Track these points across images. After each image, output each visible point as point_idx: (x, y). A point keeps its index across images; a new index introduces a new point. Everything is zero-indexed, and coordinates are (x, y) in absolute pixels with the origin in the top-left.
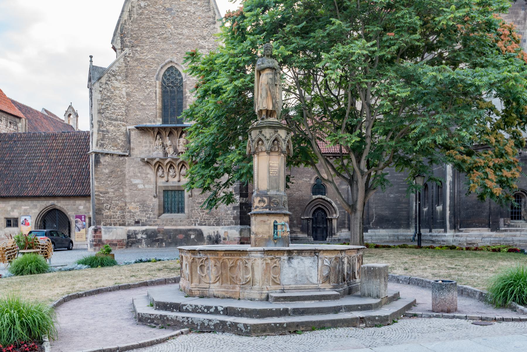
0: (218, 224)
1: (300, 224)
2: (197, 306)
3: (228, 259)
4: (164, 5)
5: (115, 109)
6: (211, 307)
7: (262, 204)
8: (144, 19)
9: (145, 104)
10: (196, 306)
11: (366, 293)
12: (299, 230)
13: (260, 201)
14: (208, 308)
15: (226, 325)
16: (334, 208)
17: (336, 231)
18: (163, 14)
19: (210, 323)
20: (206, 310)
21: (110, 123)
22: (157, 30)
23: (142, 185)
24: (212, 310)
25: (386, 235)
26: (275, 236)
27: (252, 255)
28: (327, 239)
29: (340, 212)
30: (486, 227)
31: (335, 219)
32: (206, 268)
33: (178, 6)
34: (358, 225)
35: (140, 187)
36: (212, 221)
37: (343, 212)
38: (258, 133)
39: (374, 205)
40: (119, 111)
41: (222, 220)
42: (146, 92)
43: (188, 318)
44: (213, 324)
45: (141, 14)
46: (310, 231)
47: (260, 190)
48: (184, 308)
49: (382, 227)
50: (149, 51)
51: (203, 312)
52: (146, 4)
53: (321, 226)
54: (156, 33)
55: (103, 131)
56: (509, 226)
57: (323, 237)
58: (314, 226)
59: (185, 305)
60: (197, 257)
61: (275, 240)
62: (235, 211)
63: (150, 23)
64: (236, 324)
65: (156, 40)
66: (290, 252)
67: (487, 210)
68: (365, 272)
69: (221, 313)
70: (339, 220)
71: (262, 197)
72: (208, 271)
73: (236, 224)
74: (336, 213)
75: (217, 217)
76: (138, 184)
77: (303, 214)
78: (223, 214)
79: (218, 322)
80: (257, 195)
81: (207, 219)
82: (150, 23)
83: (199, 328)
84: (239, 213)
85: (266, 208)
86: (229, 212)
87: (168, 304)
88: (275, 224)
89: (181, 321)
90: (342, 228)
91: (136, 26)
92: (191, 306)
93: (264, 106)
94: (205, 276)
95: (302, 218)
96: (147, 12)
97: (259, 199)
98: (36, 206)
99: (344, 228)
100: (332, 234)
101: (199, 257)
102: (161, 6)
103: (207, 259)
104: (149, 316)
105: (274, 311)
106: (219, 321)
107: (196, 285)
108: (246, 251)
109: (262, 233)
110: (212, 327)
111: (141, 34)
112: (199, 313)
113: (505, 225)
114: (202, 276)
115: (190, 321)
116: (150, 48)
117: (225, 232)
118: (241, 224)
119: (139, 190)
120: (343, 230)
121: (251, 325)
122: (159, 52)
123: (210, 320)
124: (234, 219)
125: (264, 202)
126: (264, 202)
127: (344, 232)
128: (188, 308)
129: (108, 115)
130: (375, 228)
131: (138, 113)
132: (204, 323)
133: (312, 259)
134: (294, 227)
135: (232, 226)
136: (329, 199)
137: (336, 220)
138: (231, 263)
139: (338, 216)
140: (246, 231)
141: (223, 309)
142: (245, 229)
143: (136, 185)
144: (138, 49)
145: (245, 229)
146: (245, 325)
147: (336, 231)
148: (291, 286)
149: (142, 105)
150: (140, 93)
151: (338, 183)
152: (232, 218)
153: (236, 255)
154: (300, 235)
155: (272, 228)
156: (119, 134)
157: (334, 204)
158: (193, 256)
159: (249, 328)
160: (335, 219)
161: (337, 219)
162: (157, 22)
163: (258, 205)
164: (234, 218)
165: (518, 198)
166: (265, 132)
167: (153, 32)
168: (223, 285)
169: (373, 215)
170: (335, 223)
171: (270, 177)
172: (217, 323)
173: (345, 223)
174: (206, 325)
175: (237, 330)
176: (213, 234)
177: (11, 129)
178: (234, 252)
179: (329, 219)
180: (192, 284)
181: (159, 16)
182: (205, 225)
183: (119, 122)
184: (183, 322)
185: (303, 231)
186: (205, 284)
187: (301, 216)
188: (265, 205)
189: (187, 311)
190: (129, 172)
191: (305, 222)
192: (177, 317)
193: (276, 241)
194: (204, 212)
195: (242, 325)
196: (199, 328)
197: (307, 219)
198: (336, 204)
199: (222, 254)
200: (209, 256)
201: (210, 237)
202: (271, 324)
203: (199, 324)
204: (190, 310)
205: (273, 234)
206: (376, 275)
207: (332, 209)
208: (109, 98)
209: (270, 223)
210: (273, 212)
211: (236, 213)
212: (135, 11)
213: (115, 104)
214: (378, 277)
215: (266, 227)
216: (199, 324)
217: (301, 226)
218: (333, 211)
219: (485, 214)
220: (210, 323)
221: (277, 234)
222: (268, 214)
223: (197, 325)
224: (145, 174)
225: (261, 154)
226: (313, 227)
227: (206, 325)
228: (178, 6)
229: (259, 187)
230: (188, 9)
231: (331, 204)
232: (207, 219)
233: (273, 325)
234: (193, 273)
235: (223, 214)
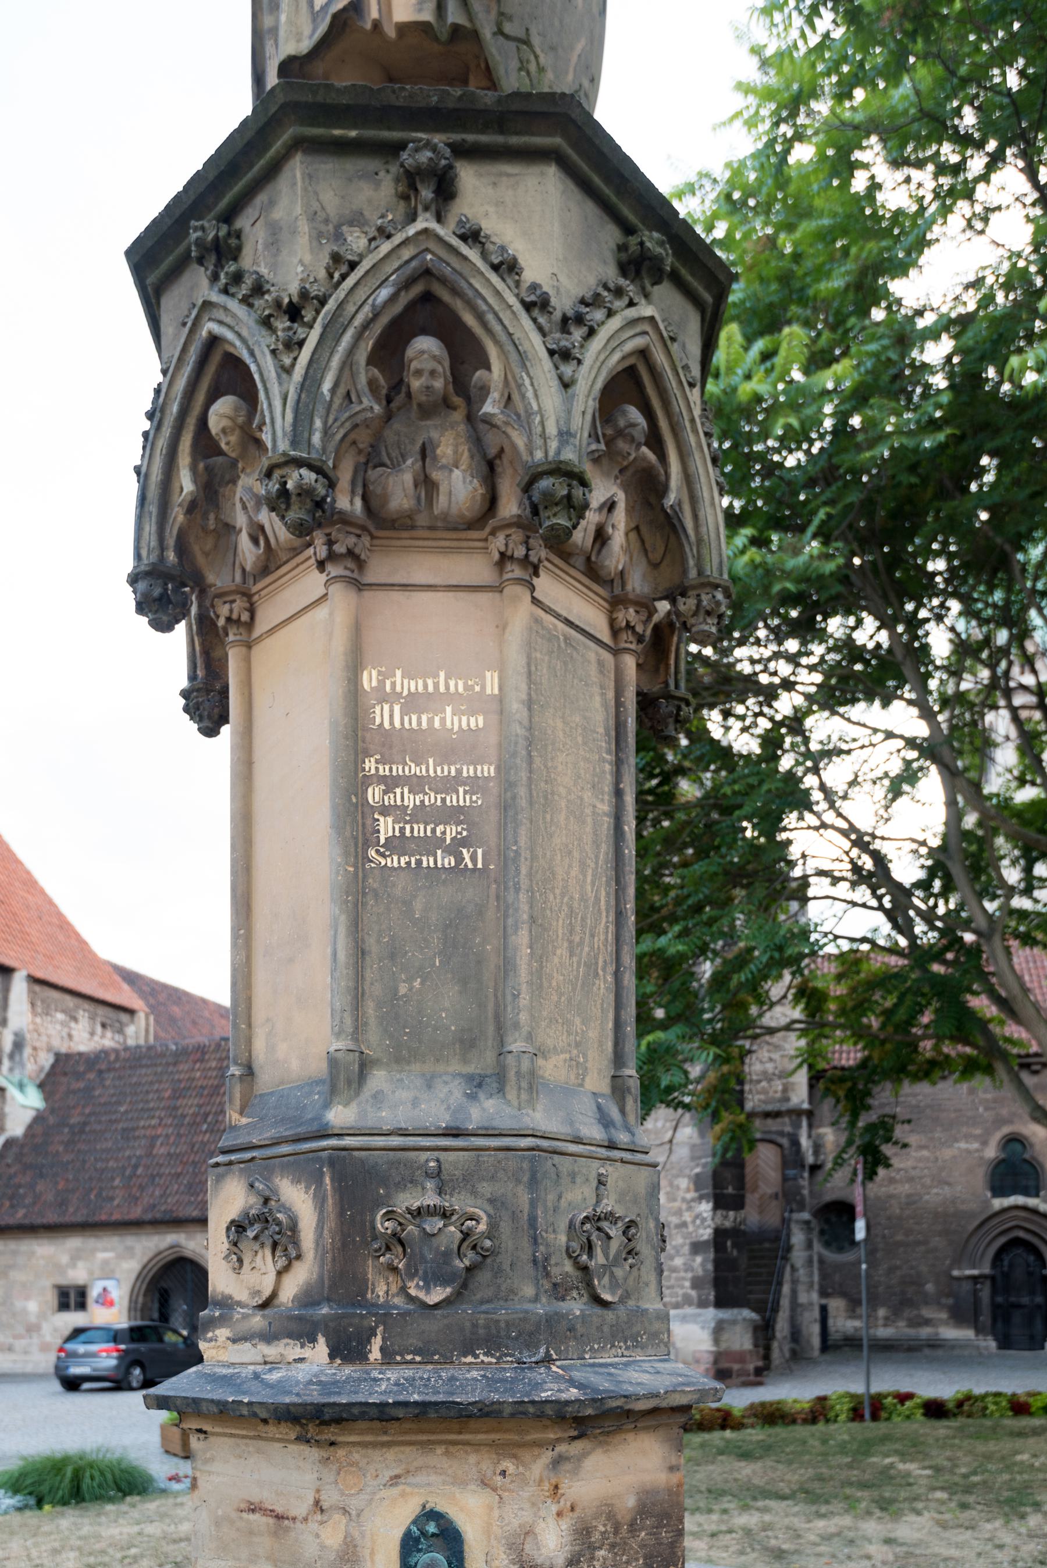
1: (948, 1296)
12: (944, 1315)
46: (985, 1318)
53: (1025, 1300)
57: (1032, 1337)
58: (999, 1299)
62: (699, 1259)
77: (957, 1262)
84: (710, 1267)
95: (956, 1273)
98: (130, 1252)
118: (720, 1303)
134: (926, 1303)
140: (738, 1329)
142: (734, 1322)
145: (734, 1322)
152: (687, 1284)
154: (950, 1333)
164: (696, 1284)
177: (108, 1041)
187: (951, 1267)
191: (967, 1286)
197: (975, 1279)
211: (703, 1264)
217: (950, 1301)
226: (995, 1307)
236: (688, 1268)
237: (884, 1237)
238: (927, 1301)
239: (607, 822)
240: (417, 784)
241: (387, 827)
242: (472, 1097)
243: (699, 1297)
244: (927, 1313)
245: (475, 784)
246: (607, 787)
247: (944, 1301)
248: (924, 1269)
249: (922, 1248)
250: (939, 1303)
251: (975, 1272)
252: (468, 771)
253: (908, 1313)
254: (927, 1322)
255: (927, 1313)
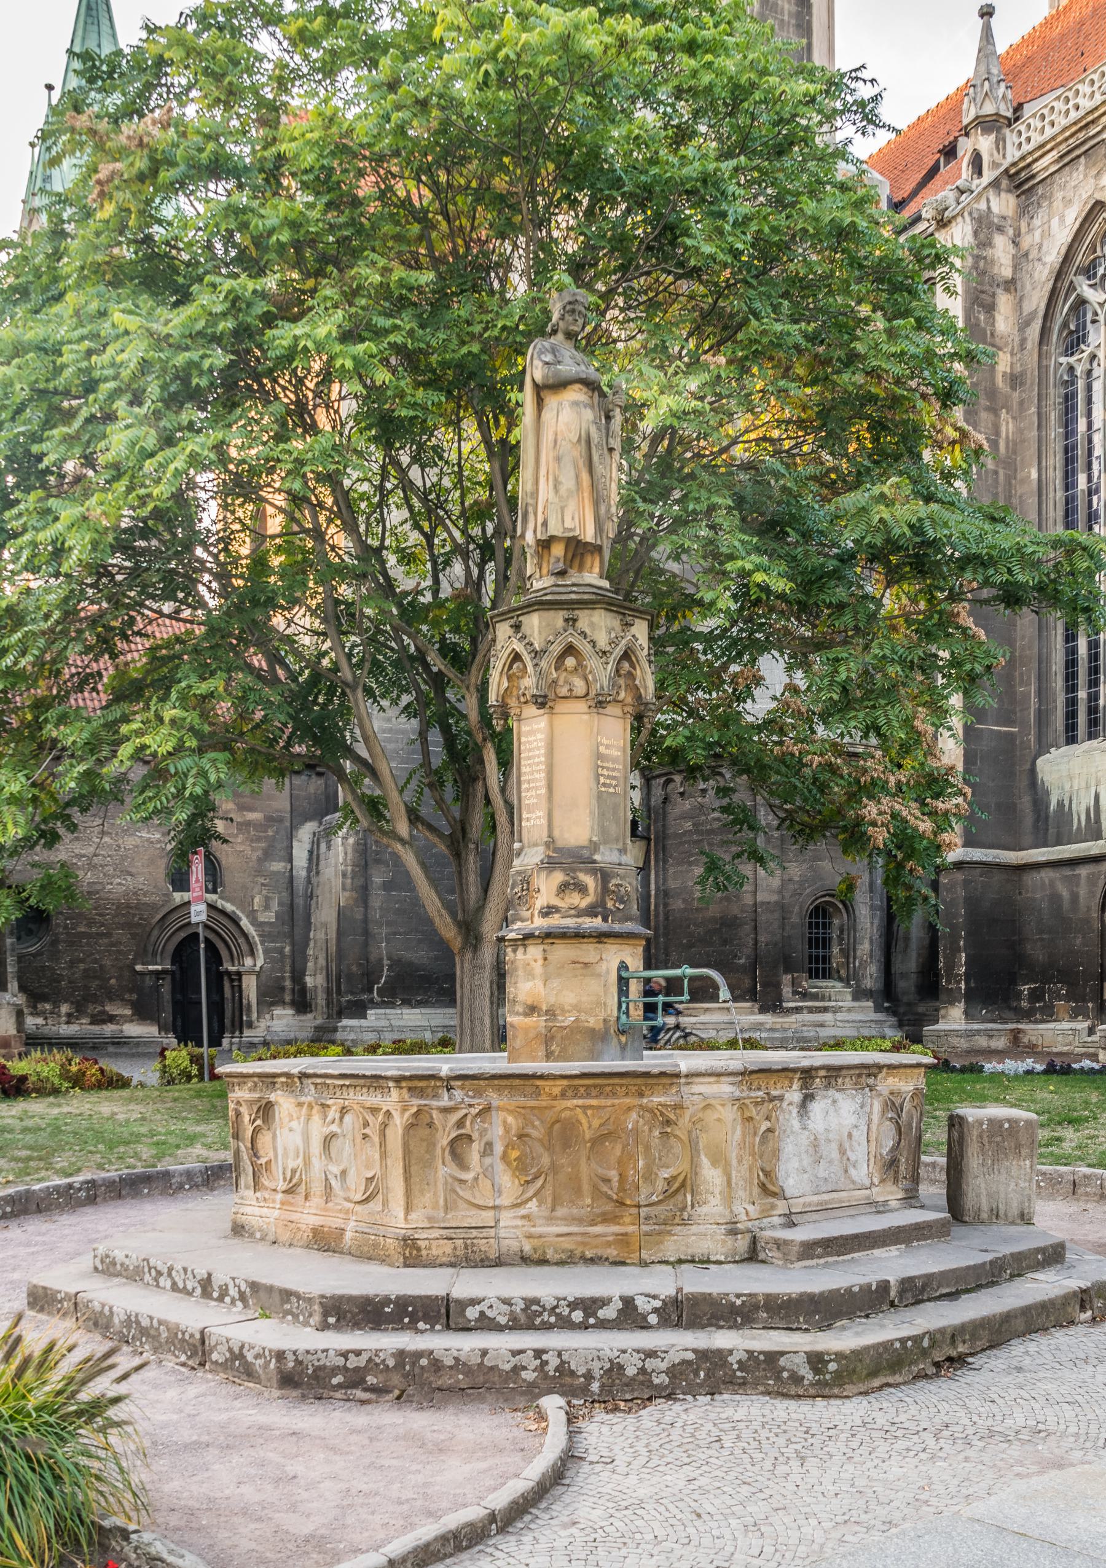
1: (131, 991)
2: (536, 1301)
3: (585, 1108)
6: (604, 1302)
7: (575, 899)
10: (530, 1302)
11: (985, 1207)
13: (563, 888)
14: (590, 1306)
15: (725, 1364)
16: (245, 935)
17: (254, 1016)
19: (650, 1364)
20: (578, 1316)
24: (609, 1313)
25: (423, 1028)
26: (623, 1017)
27: (696, 1089)
28: (225, 1042)
29: (266, 951)
30: (747, 1001)
31: (250, 973)
32: (476, 1147)
34: (487, 992)
37: (275, 950)
38: (560, 623)
39: (384, 931)
43: (539, 1353)
44: (664, 1366)
46: (166, 1015)
47: (560, 844)
48: (472, 1313)
49: (407, 1003)
51: (566, 1324)
56: (805, 996)
58: (179, 997)
59: (474, 1302)
60: (435, 1103)
61: (623, 1032)
64: (772, 1357)
66: (807, 1074)
67: (748, 951)
68: (980, 1136)
69: (653, 1319)
70: (263, 978)
71: (574, 870)
72: (488, 1160)
74: (252, 953)
79: (690, 1356)
80: (550, 864)
83: (595, 1386)
85: (591, 911)
87: (387, 1300)
88: (624, 974)
89: (507, 1367)
90: (273, 1004)
92: (507, 1302)
93: (568, 524)
94: (476, 1179)
95: (138, 968)
97: (559, 877)
99: (283, 1003)
100: (239, 1025)
101: (445, 1101)
103: (487, 1110)
104: (340, 1361)
105: (855, 1294)
106: (694, 1351)
107: (430, 1219)
108: (677, 1075)
109: (577, 1008)
110: (663, 1379)
112: (547, 1327)
113: (795, 993)
114: (462, 1182)
115: (553, 1362)
120: (278, 1011)
121: (840, 1356)
123: (651, 1354)
125: (582, 889)
126: (582, 889)
127: (280, 1017)
128: (490, 1313)
130: (390, 1005)
132: (621, 1368)
133: (859, 1099)
136: (229, 907)
137: (254, 978)
138: (596, 1123)
139: (260, 962)
141: (658, 1304)
146: (816, 1360)
147: (254, 1016)
148: (808, 1199)
151: (259, 853)
153: (621, 1091)
154: (133, 1029)
155: (614, 990)
157: (245, 923)
158: (417, 1101)
159: (832, 1367)
160: (250, 973)
161: (258, 975)
163: (556, 902)
165: (824, 917)
166: (592, 625)
168: (561, 1212)
169: (381, 960)
170: (250, 987)
171: (600, 796)
172: (684, 1362)
173: (282, 989)
174: (631, 1371)
175: (778, 1378)
178: (617, 1081)
179: (228, 973)
180: (413, 1216)
184: (517, 1369)
185: (142, 1013)
186: (474, 1212)
187: (134, 962)
188: (584, 904)
189: (486, 1324)
192: (484, 1353)
193: (623, 1039)
195: (801, 1359)
196: (595, 1386)
198: (254, 922)
199: (557, 1091)
200: (494, 1098)
202: (891, 1342)
203: (597, 1373)
204: (502, 1320)
205: (615, 1013)
206: (1018, 1146)
207: (241, 940)
209: (608, 972)
210: (617, 927)
214: (1025, 1151)
215: (594, 986)
216: (597, 1373)
217: (134, 997)
218: (245, 947)
219: (742, 961)
220: (650, 1364)
221: (627, 1013)
222: (601, 937)
223: (589, 1376)
225: (561, 707)
227: (631, 1371)
229: (556, 833)
231: (235, 922)
233: (897, 1345)
234: (414, 1169)
237: (66, 927)
238: (112, 996)
244: (112, 1009)
247: (127, 996)
248: (107, 962)
249: (106, 941)
250: (123, 1000)
251: (159, 968)
253: (92, 1008)
254: (111, 1019)
255: (112, 1009)
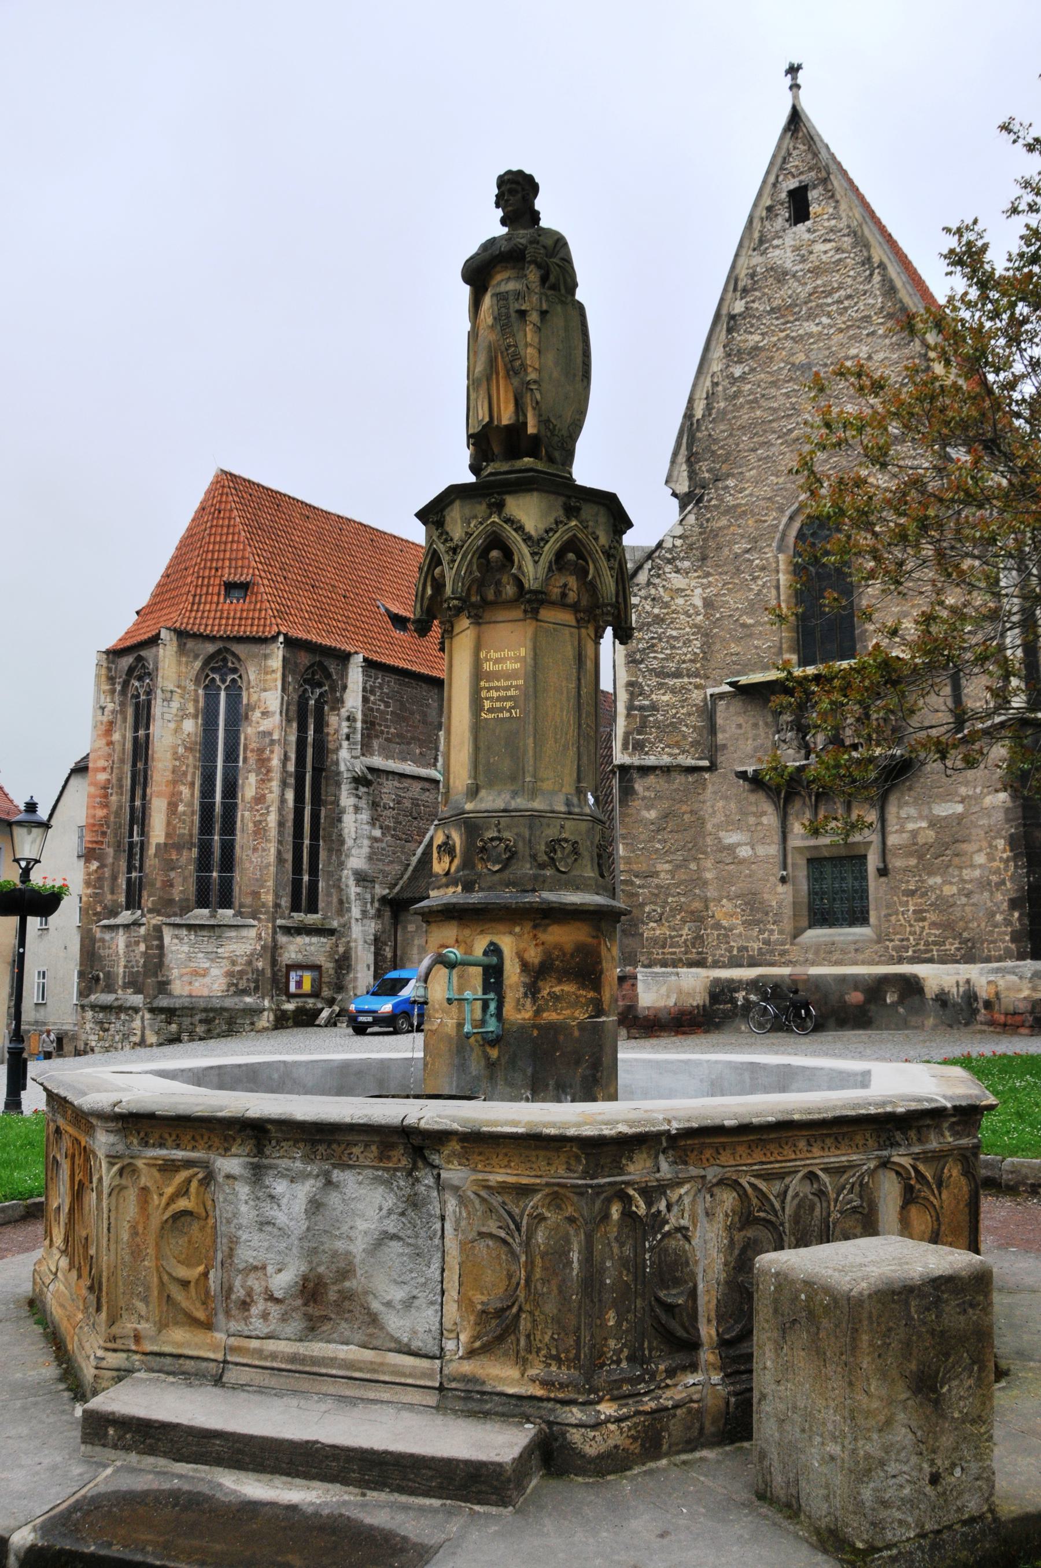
0: (969, 958)
4: (791, 360)
5: (673, 647)
8: (742, 406)
9: (750, 621)
18: (788, 381)
21: (661, 686)
22: (774, 425)
23: (748, 848)
33: (827, 353)
35: (744, 852)
36: (951, 947)
40: (685, 650)
41: (982, 944)
42: (751, 590)
45: (735, 396)
50: (757, 482)
52: (747, 369)
54: (774, 432)
55: (641, 708)
62: (1016, 915)
63: (758, 413)
65: (773, 449)
73: (1021, 957)
75: (965, 935)
76: (739, 845)
78: (983, 925)
81: (935, 943)
82: (758, 413)
84: (1026, 921)
86: (999, 918)
91: (722, 427)
96: (749, 386)
102: (782, 365)
111: (737, 445)
116: (759, 474)
117: (989, 982)
119: (742, 862)
122: (781, 480)
124: (1013, 940)
129: (655, 664)
131: (734, 648)
135: (1009, 964)
143: (731, 849)
144: (731, 483)
149: (744, 625)
150: (739, 595)
152: (1007, 938)
156: (684, 711)
162: (775, 405)
167: (765, 431)
176: (954, 990)
181: (779, 388)
182: (931, 961)
183: (686, 680)
190: (714, 812)
194: (924, 919)
201: (942, 999)
208: (659, 620)
211: (1020, 919)
212: (721, 394)
213: (674, 633)
224: (754, 814)
228: (827, 353)
230: (853, 352)
232: (935, 943)
235: (983, 925)
236: (1008, 922)
239: (574, 692)
240: (497, 689)
241: (487, 704)
242: (513, 798)
243: (1018, 949)
245: (517, 687)
246: (574, 678)
252: (514, 683)
